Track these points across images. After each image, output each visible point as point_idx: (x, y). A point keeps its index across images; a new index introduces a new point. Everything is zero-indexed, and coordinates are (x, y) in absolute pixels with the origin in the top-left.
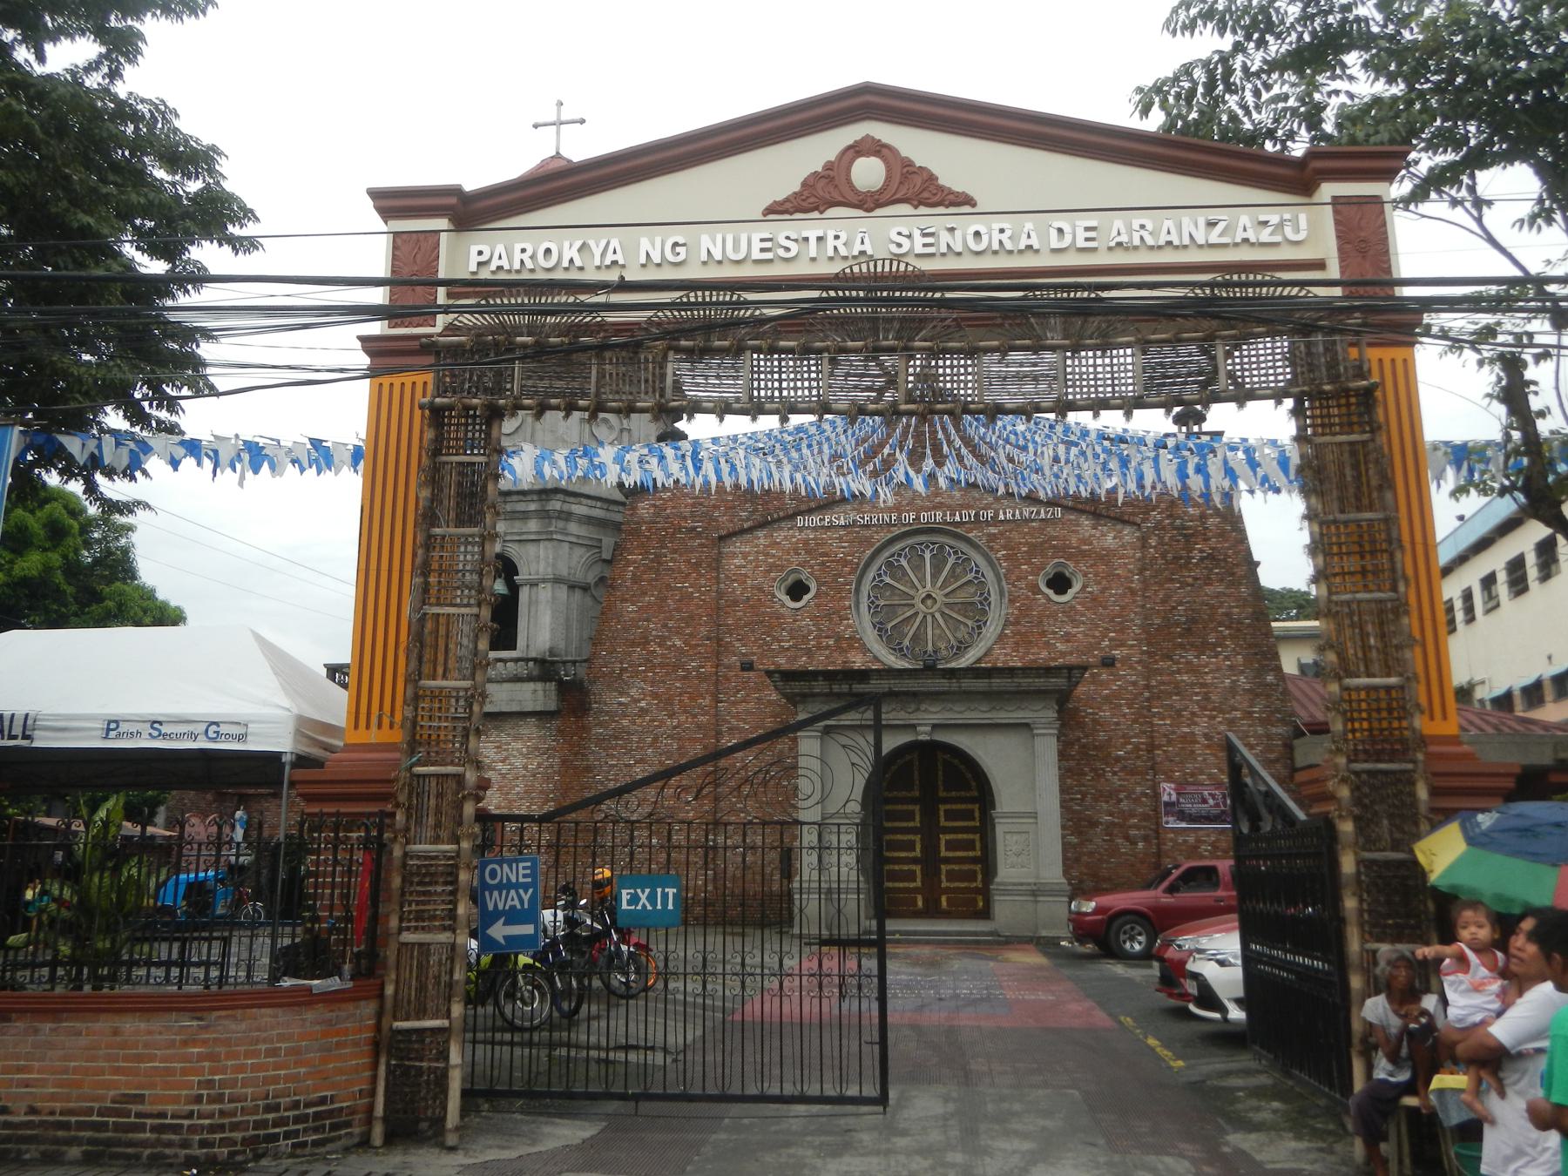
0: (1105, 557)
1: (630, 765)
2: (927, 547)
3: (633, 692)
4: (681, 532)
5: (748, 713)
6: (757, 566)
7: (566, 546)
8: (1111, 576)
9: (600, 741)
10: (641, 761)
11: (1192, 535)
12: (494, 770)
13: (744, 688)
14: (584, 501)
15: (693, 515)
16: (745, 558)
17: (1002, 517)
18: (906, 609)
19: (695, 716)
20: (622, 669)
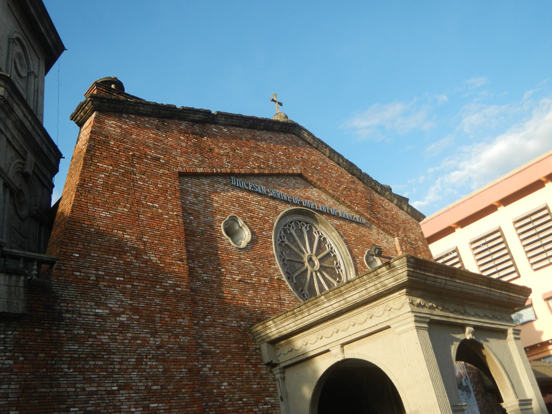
1: (112, 392)
3: (111, 304)
5: (216, 337)
6: (206, 207)
7: (5, 139)
13: (210, 313)
14: (22, 107)
16: (196, 196)
18: (300, 265)
20: (98, 277)
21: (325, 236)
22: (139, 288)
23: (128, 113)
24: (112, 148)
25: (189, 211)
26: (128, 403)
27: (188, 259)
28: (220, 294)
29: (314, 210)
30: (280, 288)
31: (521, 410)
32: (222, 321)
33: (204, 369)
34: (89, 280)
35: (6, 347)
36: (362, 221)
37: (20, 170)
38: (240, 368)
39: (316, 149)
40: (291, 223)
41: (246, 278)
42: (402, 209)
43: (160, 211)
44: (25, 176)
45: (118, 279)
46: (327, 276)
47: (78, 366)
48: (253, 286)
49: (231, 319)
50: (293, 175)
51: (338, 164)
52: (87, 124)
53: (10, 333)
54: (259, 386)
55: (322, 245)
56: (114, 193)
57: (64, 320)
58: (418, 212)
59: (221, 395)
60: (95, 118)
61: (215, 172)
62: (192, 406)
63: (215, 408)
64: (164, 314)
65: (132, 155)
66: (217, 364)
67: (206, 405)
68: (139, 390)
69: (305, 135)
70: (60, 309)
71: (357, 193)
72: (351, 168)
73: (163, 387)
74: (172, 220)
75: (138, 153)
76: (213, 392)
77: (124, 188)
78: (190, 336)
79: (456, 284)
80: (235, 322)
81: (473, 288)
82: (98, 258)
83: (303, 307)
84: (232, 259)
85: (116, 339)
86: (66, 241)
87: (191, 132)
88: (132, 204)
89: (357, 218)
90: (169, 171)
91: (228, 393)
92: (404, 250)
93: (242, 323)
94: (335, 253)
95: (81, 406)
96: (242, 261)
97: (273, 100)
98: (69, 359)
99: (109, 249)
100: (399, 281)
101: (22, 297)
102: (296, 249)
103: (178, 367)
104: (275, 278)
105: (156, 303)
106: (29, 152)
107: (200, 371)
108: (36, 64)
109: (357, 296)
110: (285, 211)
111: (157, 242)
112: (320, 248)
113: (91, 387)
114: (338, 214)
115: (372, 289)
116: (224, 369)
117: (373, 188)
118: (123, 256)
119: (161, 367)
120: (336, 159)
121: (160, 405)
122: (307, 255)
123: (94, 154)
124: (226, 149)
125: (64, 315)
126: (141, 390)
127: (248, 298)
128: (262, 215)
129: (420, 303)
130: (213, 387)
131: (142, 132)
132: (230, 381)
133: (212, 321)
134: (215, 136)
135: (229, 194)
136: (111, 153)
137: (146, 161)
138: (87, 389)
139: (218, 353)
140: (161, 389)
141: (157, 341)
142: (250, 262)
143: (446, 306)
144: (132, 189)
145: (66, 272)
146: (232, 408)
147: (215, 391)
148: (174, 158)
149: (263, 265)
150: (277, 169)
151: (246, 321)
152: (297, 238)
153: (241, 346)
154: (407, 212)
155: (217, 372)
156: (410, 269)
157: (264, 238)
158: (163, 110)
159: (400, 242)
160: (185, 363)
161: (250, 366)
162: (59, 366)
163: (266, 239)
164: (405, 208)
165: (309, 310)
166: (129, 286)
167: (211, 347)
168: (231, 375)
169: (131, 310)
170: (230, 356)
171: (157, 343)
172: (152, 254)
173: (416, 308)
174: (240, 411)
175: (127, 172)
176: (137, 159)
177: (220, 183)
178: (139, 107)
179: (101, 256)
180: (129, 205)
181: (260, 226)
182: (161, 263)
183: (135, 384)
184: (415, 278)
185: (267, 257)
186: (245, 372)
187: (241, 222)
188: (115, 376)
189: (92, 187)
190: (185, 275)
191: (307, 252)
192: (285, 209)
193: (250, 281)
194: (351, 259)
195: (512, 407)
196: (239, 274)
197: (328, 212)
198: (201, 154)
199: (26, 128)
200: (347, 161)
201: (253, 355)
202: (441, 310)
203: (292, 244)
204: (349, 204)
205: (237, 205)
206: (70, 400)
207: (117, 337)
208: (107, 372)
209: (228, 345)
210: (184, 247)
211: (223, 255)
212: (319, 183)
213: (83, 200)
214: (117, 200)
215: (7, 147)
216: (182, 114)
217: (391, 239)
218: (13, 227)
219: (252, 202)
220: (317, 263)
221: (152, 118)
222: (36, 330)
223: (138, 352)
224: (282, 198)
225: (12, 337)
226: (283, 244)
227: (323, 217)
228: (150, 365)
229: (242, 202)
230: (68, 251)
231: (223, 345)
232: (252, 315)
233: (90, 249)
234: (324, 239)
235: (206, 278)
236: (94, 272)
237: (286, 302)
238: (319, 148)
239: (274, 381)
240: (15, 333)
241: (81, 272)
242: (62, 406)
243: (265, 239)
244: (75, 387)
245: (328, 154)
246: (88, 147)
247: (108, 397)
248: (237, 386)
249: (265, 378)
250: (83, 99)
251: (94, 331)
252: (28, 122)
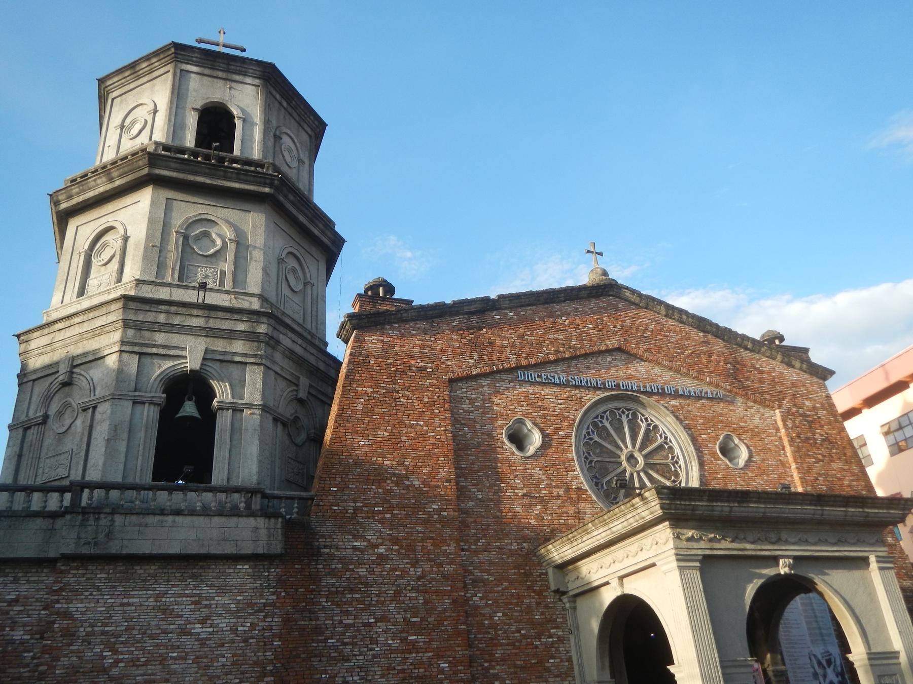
0: (756, 433)
1: (370, 625)
2: (623, 413)
4: (411, 370)
5: (491, 563)
6: (484, 413)
7: (272, 373)
8: (765, 450)
9: (332, 595)
10: (383, 619)
11: (812, 421)
12: (191, 634)
13: (484, 536)
14: (290, 334)
15: (422, 356)
17: (681, 392)
18: (615, 466)
19: (440, 565)
21: (657, 423)
22: (400, 516)
23: (390, 323)
24: (372, 368)
25: (463, 422)
26: (385, 635)
27: (458, 476)
28: (498, 514)
29: (639, 391)
30: (580, 499)
31: (871, 665)
32: (499, 544)
33: (475, 599)
34: (347, 513)
35: (270, 584)
36: (717, 394)
37: (295, 396)
38: (520, 597)
39: (646, 308)
40: (605, 412)
41: (533, 492)
42: (793, 367)
43: (425, 428)
44: (301, 401)
45: (376, 509)
46: (655, 475)
47: (335, 600)
48: (542, 500)
49: (510, 541)
50: (609, 351)
51: (681, 322)
52: (350, 343)
53: (273, 570)
54: (542, 617)
55: (652, 436)
56: (374, 417)
57: (323, 556)
58: (821, 367)
59: (494, 626)
60: (355, 337)
61: (495, 369)
63: (485, 641)
64: (426, 542)
65: (394, 371)
66: (490, 593)
68: (397, 622)
69: (627, 294)
70: (319, 545)
71: (711, 357)
72: (701, 324)
73: (422, 619)
74: (439, 437)
75: (401, 367)
76: (484, 623)
77: (385, 410)
78: (455, 565)
79: (750, 509)
80: (515, 544)
81: (787, 510)
82: (356, 490)
83: (575, 533)
84: (515, 471)
85: (373, 571)
86: (325, 476)
87: (466, 327)
88: (393, 426)
89: (709, 392)
90: (437, 380)
92: (790, 426)
93: (524, 544)
94: (671, 444)
95: (338, 637)
96: (530, 471)
97: (589, 252)
98: (327, 593)
99: (368, 479)
100: (655, 514)
101: (280, 538)
102: (609, 447)
103: (441, 598)
104: (574, 487)
105: (417, 531)
106: (302, 377)
107: (469, 601)
108: (314, 268)
109: (619, 527)
110: (594, 400)
111: (420, 464)
112: (647, 439)
113: (348, 619)
114: (677, 391)
115: (632, 520)
116: (498, 598)
117: (740, 345)
118: (383, 484)
119: (422, 598)
120: (676, 316)
121: (419, 637)
122: (625, 451)
123: (354, 379)
124: (511, 338)
125: (322, 551)
126: (399, 622)
127: (534, 514)
128: (559, 411)
129: (693, 536)
131: (406, 341)
133: (486, 545)
134: (497, 325)
135: (516, 392)
136: (371, 373)
137: (410, 374)
138: (344, 622)
139: (492, 581)
140: (421, 621)
141: (418, 572)
142: (539, 472)
143: (741, 536)
144: (393, 409)
145: (324, 507)
147: (486, 622)
148: (444, 363)
149: (558, 473)
150: (583, 348)
151: (530, 542)
152: (612, 432)
153: (522, 571)
154: (801, 369)
155: (491, 602)
156: (664, 502)
157: (560, 440)
158: (430, 310)
159: (782, 416)
161: (533, 594)
162: (318, 600)
163: (564, 440)
164: (797, 364)
165: (582, 537)
166: (389, 516)
167: (483, 574)
168: (507, 604)
169: (390, 540)
170: (507, 584)
171: (418, 574)
172: (415, 478)
173: (685, 542)
174: (517, 644)
175: (388, 391)
176: (400, 374)
177: (503, 381)
178: (401, 314)
179: (360, 487)
180: (390, 428)
181: (556, 426)
182: (424, 487)
183: (393, 616)
184: (674, 510)
185: (564, 463)
186: (525, 601)
187: (529, 424)
188: (372, 609)
189: (351, 415)
190: (453, 497)
191: (627, 447)
192: (591, 398)
193: (537, 495)
194: (693, 450)
195: (860, 660)
196: (524, 487)
197: (660, 391)
198: (478, 352)
199: (296, 354)
200: (694, 316)
201: (537, 581)
202: (733, 541)
203: (604, 440)
204: (696, 374)
205: (525, 404)
206: (327, 632)
207: (375, 569)
208: (365, 604)
209: (505, 571)
210: (452, 466)
211: (503, 467)
212: (646, 355)
213: (341, 430)
214: (377, 425)
215: (276, 379)
216: (453, 309)
217: (768, 413)
218: (288, 457)
219: (546, 397)
220: (641, 460)
221: (418, 322)
222: (296, 566)
223: (397, 583)
224: (589, 385)
225: (274, 574)
226: (592, 442)
227: (651, 400)
228: (410, 597)
229: (533, 398)
230: (326, 485)
231: (499, 571)
232: (539, 534)
233: (348, 481)
234: (656, 427)
235: (480, 497)
236: (352, 504)
237: (587, 516)
238: (650, 307)
239: (563, 610)
240: (277, 570)
241: (338, 506)
242: (320, 638)
243: (563, 440)
244: (333, 620)
245: (663, 312)
246: (347, 372)
247: (365, 629)
248: (514, 617)
249: (552, 608)
250: (343, 319)
251: (351, 565)
252: (298, 346)
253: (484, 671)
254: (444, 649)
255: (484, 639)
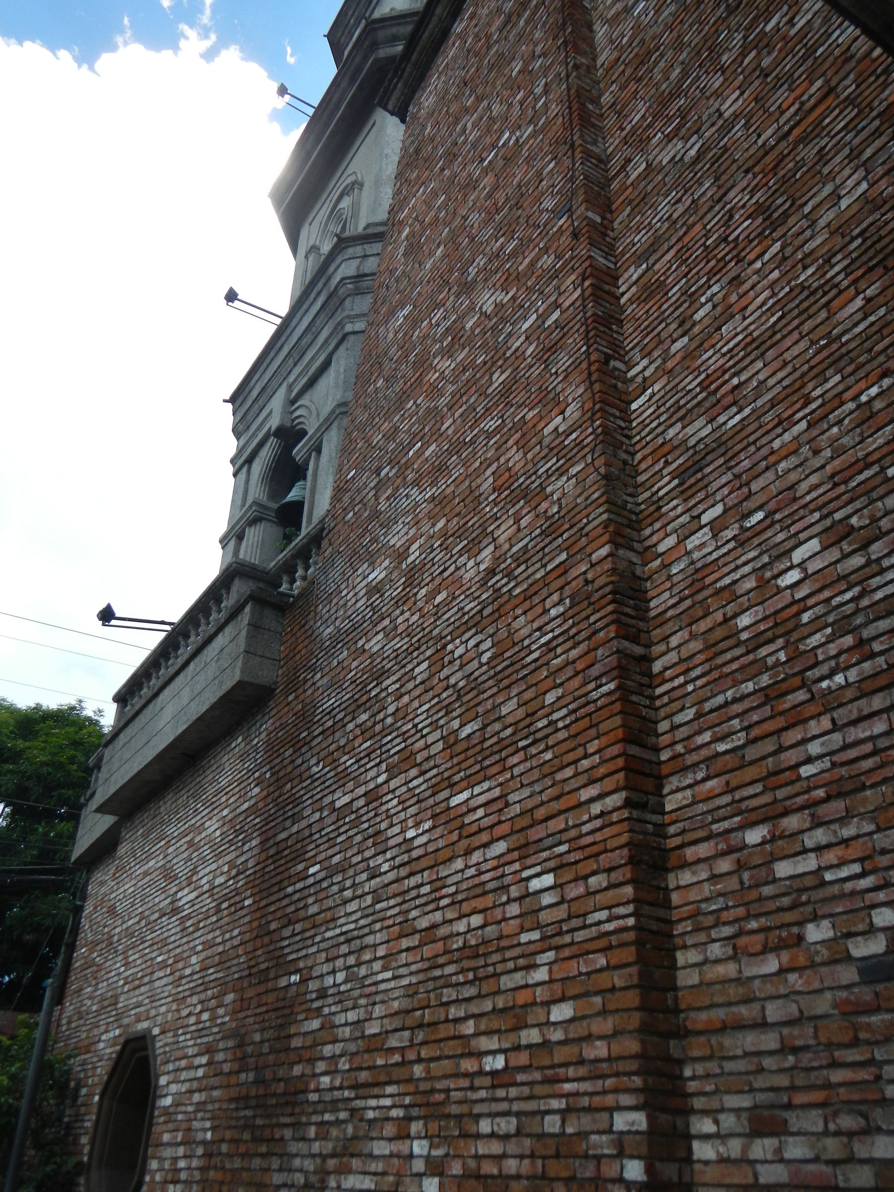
62: (580, 751)
67: (699, 716)
91: (827, 594)
116: (793, 477)
121: (477, 790)
130: (730, 609)
132: (838, 516)
133: (725, 298)
146: (853, 675)
155: (760, 515)
160: (560, 582)
231: (787, 356)
253: (746, 876)
254: (540, 813)
255: (737, 708)
